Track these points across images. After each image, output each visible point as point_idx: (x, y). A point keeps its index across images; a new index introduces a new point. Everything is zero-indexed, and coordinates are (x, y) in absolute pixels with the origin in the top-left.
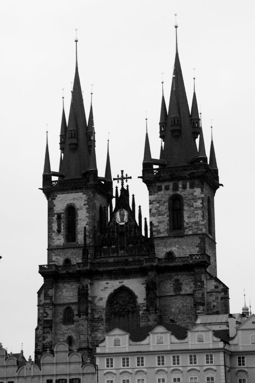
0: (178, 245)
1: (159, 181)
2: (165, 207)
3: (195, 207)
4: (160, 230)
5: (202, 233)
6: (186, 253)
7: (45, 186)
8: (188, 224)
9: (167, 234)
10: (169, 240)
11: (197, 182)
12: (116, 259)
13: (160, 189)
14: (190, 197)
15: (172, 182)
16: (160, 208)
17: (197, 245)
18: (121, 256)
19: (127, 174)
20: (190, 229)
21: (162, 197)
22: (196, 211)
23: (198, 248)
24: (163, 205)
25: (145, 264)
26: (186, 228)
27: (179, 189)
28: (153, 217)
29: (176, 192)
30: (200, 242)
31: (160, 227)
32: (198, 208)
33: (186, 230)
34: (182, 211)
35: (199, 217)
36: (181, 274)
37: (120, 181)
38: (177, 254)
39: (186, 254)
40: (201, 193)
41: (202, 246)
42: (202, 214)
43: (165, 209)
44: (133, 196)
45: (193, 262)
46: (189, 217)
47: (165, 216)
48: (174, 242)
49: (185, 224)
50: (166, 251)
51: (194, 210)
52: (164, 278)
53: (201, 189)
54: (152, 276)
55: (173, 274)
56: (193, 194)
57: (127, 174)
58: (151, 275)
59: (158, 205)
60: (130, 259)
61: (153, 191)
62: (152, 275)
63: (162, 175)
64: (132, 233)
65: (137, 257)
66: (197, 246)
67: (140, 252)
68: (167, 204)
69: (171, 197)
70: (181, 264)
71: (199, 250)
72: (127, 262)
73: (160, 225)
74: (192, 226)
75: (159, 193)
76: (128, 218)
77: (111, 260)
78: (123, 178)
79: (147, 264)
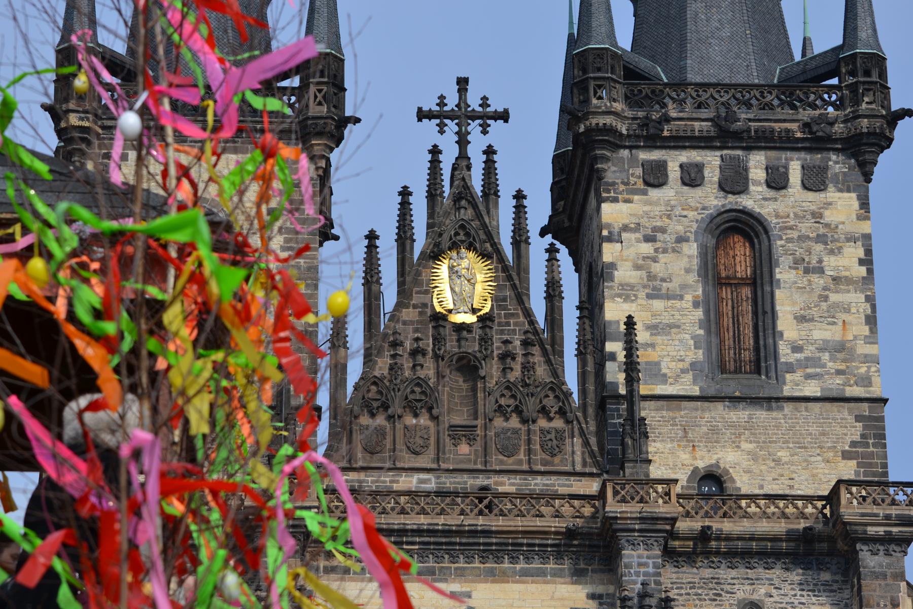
0: (751, 442)
1: (654, 140)
2: (686, 259)
3: (831, 273)
4: (658, 364)
5: (868, 396)
6: (791, 482)
7: (74, 101)
8: (797, 349)
9: (697, 388)
10: (707, 415)
11: (837, 164)
12: (431, 483)
13: (655, 177)
14: (807, 227)
15: (718, 153)
16: (656, 264)
17: (847, 448)
18: (454, 470)
19: (484, 99)
20: (809, 371)
21: (669, 217)
22: (837, 292)
23: (855, 462)
24: (674, 250)
25: (613, 507)
26: (790, 368)
27: (752, 188)
28: (625, 301)
29: (739, 200)
30: (863, 436)
31: (657, 349)
32: (849, 281)
33: (788, 377)
34: (767, 288)
35: (851, 324)
36: (772, 580)
37: (452, 126)
38: (743, 483)
39: (791, 487)
40: (860, 218)
41: (871, 455)
42: (869, 311)
43: (683, 272)
44: (519, 196)
45: (863, 515)
46: (801, 319)
47: (684, 304)
48: (732, 425)
49: (784, 349)
50: (691, 462)
51: (825, 289)
52: (683, 592)
53: (859, 198)
54: (642, 570)
55: (725, 573)
56: (821, 216)
57: (484, 99)
58: (640, 565)
59: (647, 248)
60: (507, 485)
61: (623, 183)
62: (645, 565)
63: (673, 114)
64: (517, 367)
65: (538, 483)
66: (846, 455)
67: (557, 460)
68: (692, 249)
69: (712, 218)
70: (780, 527)
71: (857, 473)
72: (485, 500)
73: (659, 339)
74: (820, 358)
75: (654, 193)
76: (495, 299)
77: (411, 482)
78: (462, 113)
79: (624, 508)
